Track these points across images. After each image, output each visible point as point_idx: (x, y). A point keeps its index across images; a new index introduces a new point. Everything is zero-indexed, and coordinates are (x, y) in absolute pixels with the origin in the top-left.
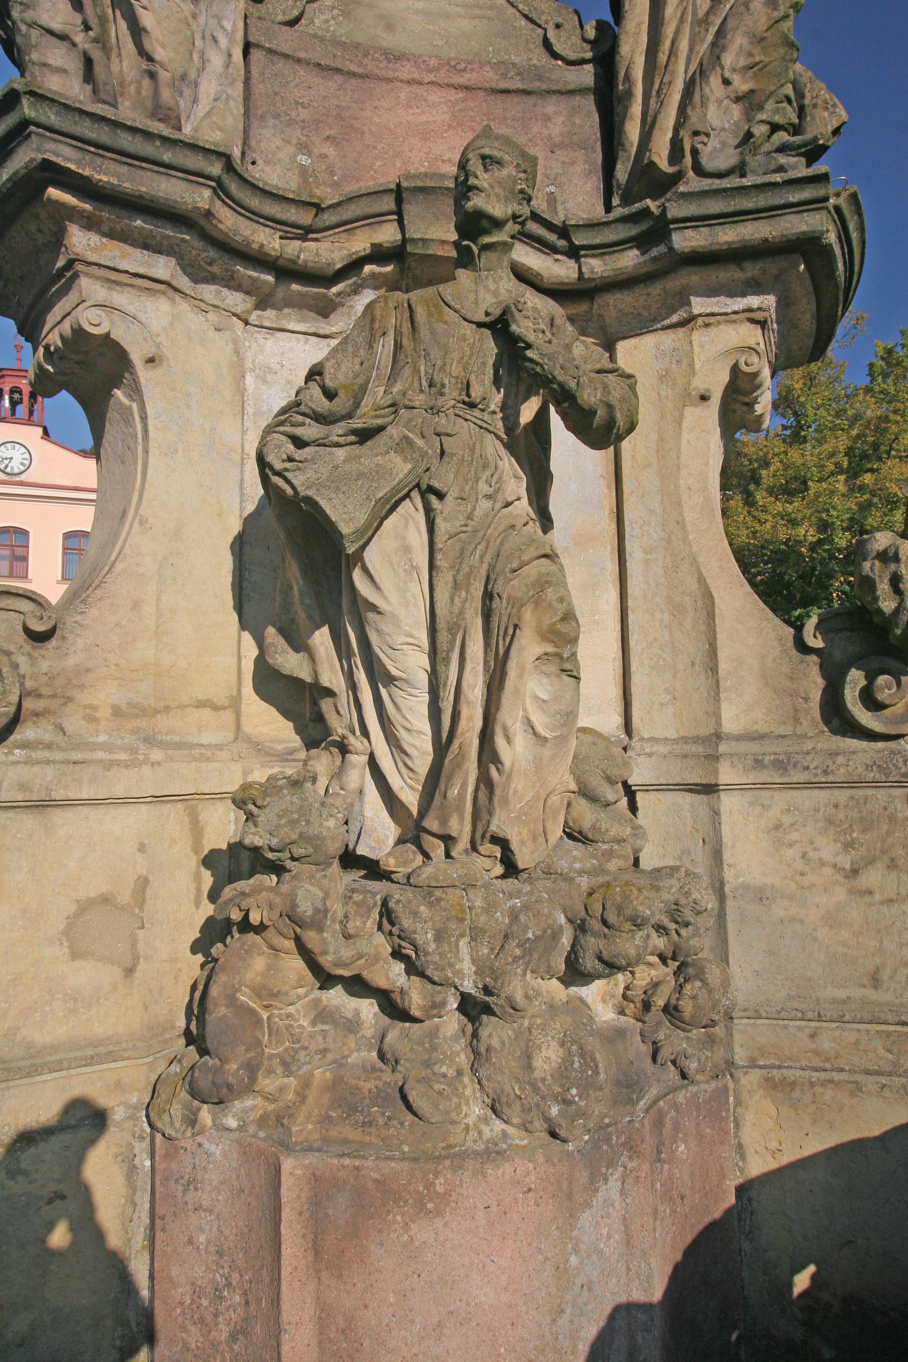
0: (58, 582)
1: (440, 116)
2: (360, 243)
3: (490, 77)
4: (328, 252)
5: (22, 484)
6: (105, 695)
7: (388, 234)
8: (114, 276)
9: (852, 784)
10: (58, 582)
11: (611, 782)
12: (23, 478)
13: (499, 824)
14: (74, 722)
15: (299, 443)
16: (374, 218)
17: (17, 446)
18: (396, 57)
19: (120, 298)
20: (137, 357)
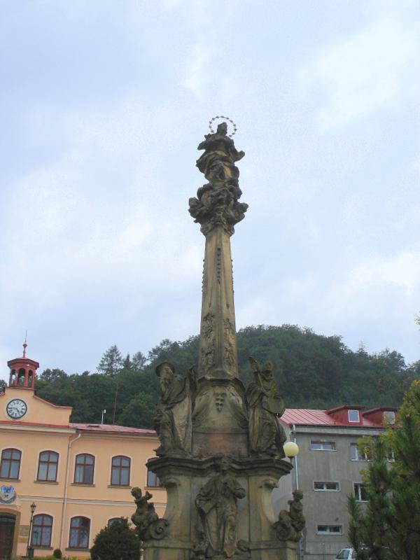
0: (35, 482)
1: (222, 438)
2: (208, 465)
4: (204, 467)
5: (21, 423)
6: (173, 533)
7: (212, 463)
8: (175, 474)
9: (279, 548)
10: (35, 482)
11: (245, 548)
12: (21, 420)
13: (225, 550)
14: (170, 537)
15: (200, 500)
16: (211, 462)
17: (20, 402)
18: (214, 430)
19: (177, 477)
20: (177, 484)
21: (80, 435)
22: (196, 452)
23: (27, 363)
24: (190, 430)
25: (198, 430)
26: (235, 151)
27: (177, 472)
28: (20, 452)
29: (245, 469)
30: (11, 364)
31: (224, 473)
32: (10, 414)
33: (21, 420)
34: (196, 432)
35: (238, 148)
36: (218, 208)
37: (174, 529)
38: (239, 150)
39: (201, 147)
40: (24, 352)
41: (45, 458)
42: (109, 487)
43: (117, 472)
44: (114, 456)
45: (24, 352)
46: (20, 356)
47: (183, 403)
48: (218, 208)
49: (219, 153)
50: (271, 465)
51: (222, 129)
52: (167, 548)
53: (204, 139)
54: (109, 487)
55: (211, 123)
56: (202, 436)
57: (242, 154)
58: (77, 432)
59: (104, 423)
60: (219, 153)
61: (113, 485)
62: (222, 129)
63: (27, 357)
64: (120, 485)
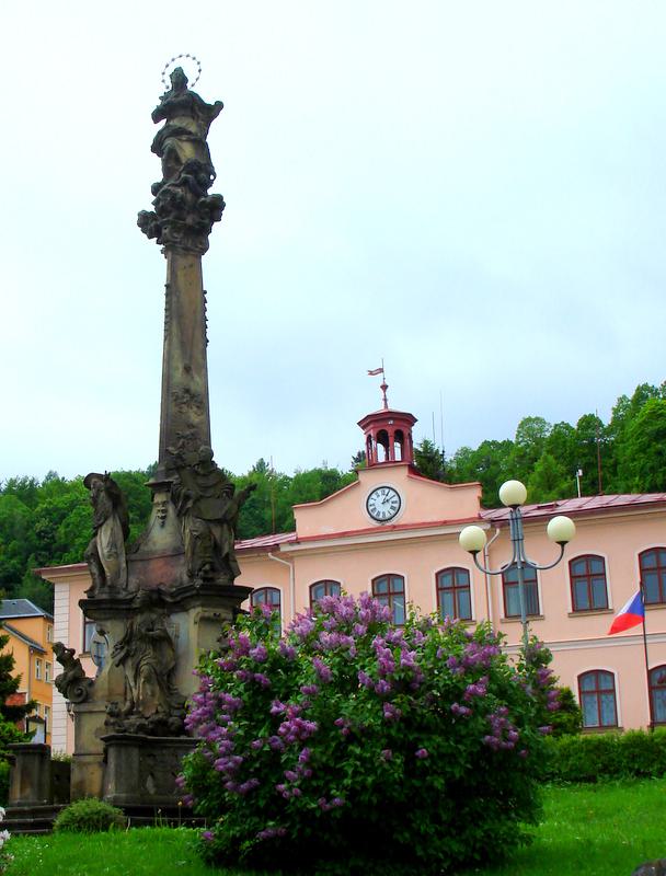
3: (170, 553)
6: (100, 694)
12: (394, 522)
21: (498, 531)
22: (132, 587)
23: (390, 419)
24: (123, 559)
25: (133, 557)
26: (209, 107)
27: (103, 616)
28: (602, 559)
29: (179, 602)
30: (365, 423)
31: (139, 611)
32: (374, 514)
33: (394, 522)
34: (132, 561)
35: (209, 100)
36: (184, 214)
37: (101, 690)
38: (213, 104)
39: (156, 117)
40: (385, 400)
41: (447, 582)
42: (570, 615)
43: (582, 587)
44: (373, 577)
45: (385, 400)
46: (378, 408)
47: (104, 526)
48: (184, 214)
49: (184, 116)
50: (194, 592)
51: (179, 79)
52: (91, 712)
53: (159, 102)
54: (570, 615)
55: (188, 56)
56: (140, 565)
57: (219, 106)
58: (492, 526)
59: (582, 496)
60: (184, 116)
61: (577, 610)
62: (179, 79)
63: (394, 407)
64: (591, 610)
